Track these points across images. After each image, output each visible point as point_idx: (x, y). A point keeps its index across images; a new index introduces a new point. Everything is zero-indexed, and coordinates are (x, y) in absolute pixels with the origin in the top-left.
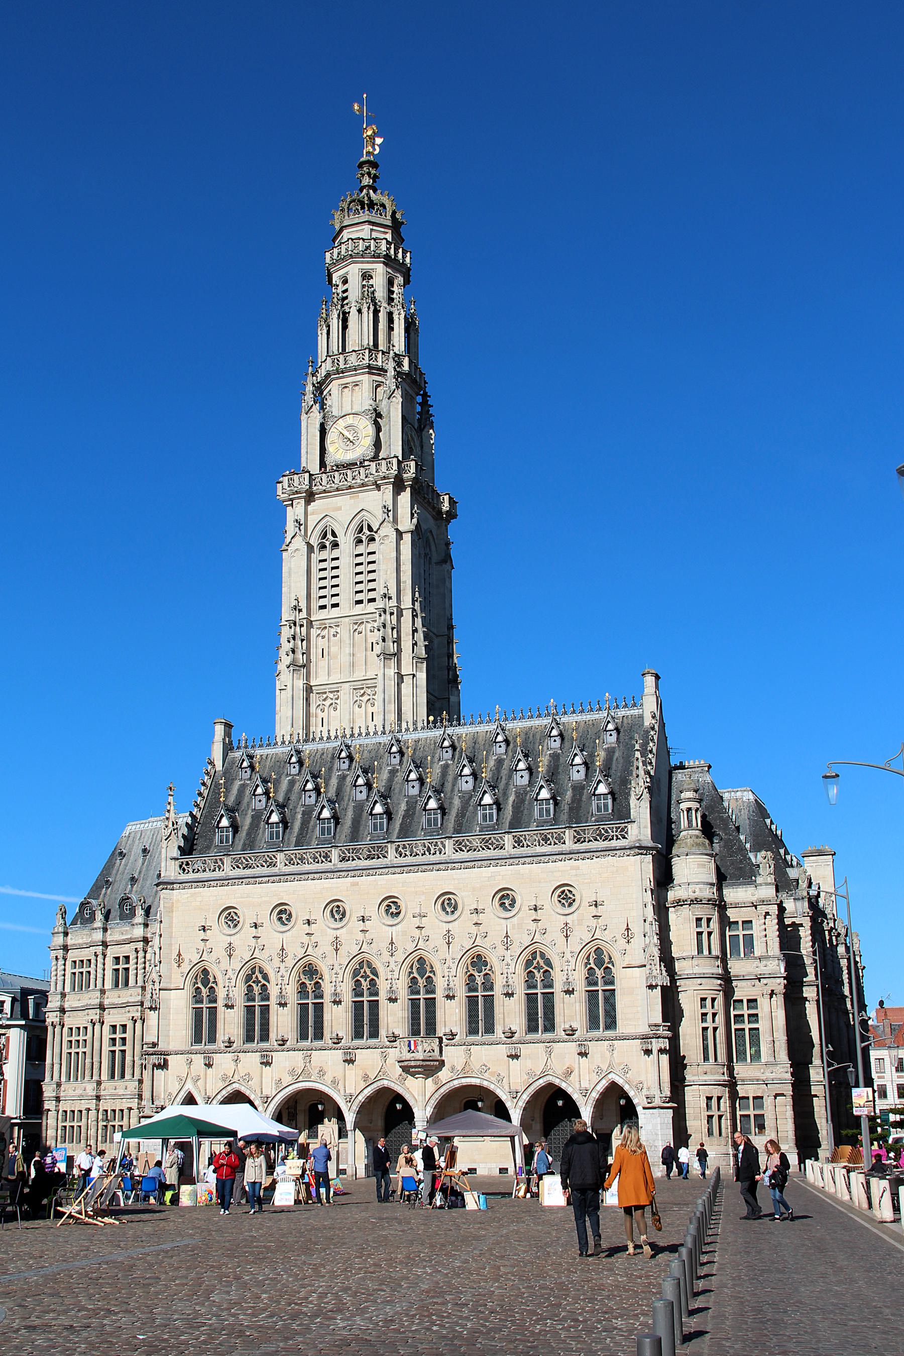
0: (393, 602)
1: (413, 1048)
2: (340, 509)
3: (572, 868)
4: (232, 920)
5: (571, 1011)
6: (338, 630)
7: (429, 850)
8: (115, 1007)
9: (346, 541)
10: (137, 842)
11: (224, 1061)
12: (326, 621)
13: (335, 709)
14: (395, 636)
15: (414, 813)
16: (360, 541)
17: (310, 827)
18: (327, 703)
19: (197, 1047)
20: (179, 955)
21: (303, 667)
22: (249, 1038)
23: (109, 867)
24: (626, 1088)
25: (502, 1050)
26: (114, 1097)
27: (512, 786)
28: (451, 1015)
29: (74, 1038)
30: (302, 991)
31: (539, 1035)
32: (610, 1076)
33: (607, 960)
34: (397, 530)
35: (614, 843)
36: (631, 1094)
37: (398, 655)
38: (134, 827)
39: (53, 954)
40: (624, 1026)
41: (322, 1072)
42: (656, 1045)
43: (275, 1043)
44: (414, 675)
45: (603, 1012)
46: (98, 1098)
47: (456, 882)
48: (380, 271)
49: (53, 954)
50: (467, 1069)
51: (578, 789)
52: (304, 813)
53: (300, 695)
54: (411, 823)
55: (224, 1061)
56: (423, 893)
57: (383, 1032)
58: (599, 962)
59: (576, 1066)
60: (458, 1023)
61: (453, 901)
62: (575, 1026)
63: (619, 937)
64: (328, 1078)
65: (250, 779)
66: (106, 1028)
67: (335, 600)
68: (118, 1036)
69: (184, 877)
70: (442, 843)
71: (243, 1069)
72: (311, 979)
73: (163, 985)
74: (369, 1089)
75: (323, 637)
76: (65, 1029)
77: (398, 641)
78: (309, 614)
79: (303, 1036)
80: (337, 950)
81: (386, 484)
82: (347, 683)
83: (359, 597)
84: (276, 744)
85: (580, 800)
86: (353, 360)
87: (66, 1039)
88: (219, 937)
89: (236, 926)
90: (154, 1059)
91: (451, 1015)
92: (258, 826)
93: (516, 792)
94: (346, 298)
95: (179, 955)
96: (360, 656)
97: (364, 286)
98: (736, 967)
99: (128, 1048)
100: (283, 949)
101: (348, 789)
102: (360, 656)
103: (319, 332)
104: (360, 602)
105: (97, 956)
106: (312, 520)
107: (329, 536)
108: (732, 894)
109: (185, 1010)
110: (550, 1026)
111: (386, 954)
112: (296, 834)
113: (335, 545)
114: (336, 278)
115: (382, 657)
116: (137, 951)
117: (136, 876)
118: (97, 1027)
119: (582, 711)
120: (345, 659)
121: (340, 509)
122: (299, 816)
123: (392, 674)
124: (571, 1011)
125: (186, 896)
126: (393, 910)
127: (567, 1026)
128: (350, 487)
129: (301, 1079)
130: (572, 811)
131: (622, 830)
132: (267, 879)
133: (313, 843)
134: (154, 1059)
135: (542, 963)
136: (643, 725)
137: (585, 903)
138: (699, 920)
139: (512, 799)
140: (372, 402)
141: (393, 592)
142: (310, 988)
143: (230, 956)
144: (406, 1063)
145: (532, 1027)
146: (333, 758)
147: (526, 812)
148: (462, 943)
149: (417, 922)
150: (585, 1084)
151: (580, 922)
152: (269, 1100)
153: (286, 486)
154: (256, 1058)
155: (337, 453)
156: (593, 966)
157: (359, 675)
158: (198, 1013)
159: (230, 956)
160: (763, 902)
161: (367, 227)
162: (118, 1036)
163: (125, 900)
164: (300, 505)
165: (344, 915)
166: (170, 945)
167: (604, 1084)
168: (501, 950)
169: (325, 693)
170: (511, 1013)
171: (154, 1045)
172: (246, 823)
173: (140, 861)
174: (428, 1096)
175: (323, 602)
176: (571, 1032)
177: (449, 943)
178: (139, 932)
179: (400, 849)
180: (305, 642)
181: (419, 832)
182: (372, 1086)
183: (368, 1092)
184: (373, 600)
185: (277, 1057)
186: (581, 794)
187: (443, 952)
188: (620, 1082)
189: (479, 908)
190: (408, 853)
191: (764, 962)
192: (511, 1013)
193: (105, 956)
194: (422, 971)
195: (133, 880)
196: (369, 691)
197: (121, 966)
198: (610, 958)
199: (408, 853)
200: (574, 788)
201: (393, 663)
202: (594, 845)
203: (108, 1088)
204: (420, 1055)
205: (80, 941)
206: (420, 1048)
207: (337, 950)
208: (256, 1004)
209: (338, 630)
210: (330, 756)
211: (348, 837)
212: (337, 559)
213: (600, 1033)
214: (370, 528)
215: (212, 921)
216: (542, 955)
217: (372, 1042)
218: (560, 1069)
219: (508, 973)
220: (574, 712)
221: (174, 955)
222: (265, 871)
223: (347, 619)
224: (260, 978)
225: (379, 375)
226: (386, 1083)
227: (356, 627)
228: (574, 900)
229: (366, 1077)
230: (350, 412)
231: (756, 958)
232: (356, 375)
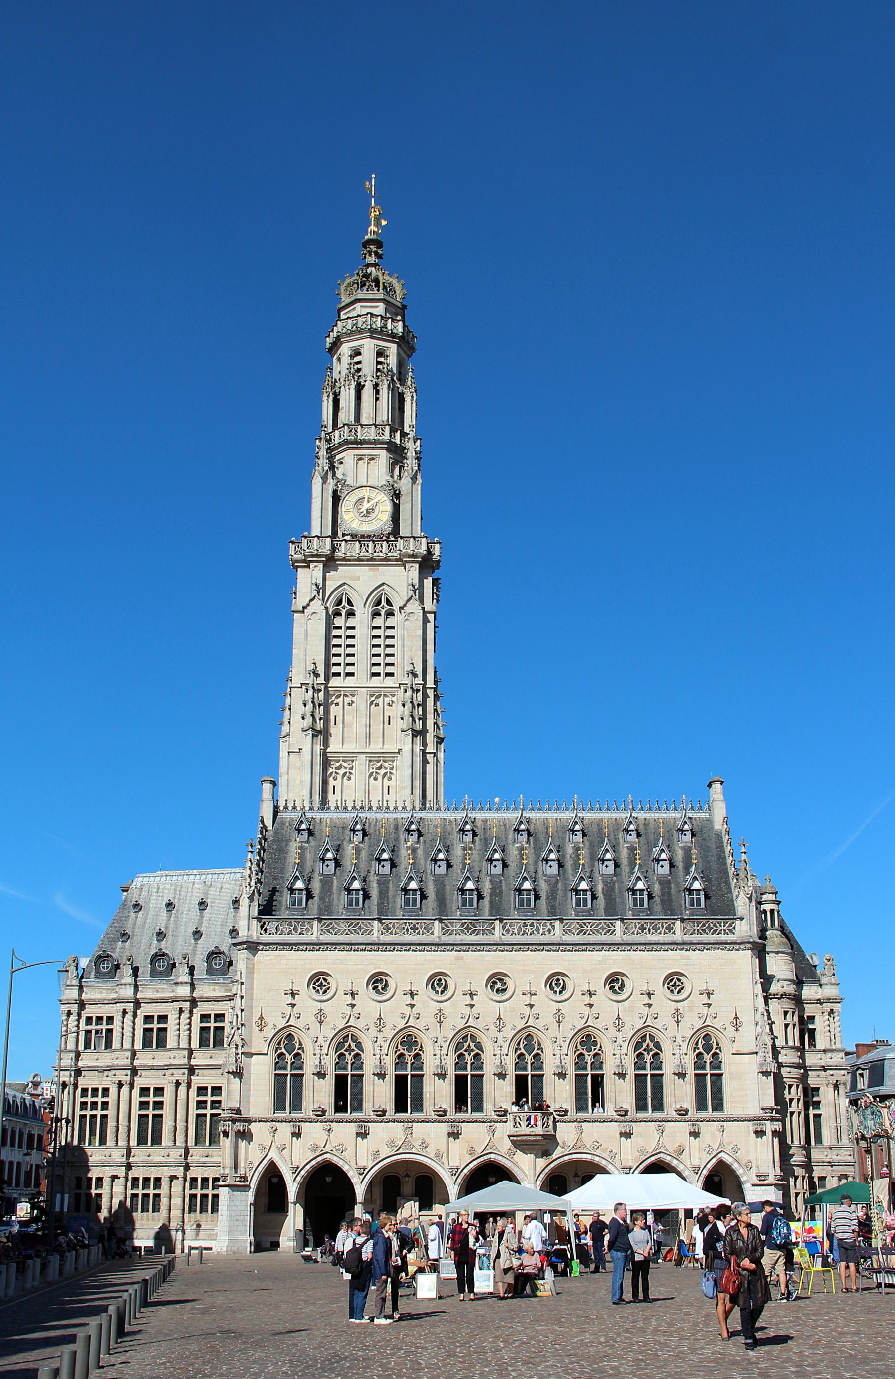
0: (419, 680)
1: (532, 1123)
2: (358, 578)
3: (683, 957)
4: (321, 985)
5: (679, 1093)
6: (354, 699)
7: (538, 930)
8: (152, 1068)
9: (363, 613)
10: (154, 896)
11: (314, 1132)
12: (341, 689)
13: (349, 779)
14: (420, 713)
15: (501, 892)
16: (376, 614)
17: (390, 897)
18: (341, 771)
19: (280, 1115)
20: (261, 1018)
21: (322, 734)
22: (340, 1108)
23: (122, 918)
24: (735, 1166)
25: (615, 1128)
26: (148, 1165)
27: (597, 874)
28: (559, 1093)
29: (89, 1100)
30: (400, 1060)
31: (649, 1114)
32: (720, 1155)
33: (715, 1046)
34: (423, 609)
35: (723, 937)
36: (740, 1171)
37: (423, 733)
38: (146, 879)
39: (65, 1008)
40: (730, 1108)
41: (424, 1145)
42: (769, 1127)
43: (372, 1114)
45: (710, 1092)
46: (129, 1167)
47: (566, 962)
48: (393, 349)
49: (65, 1008)
50: (579, 1144)
51: (665, 883)
52: (379, 881)
53: (318, 760)
54: (500, 902)
55: (314, 1132)
56: (533, 972)
57: (488, 1106)
58: (708, 1047)
59: (687, 1143)
60: (569, 1100)
61: (561, 981)
62: (685, 1106)
63: (728, 1025)
64: (431, 1151)
65: (308, 842)
66: (136, 1092)
67: (349, 669)
68: (151, 1099)
69: (265, 938)
70: (551, 924)
71: (335, 1140)
72: (409, 1050)
73: (245, 1049)
74: (475, 1162)
76: (79, 1091)
77: (424, 719)
78: (327, 679)
79: (401, 1106)
80: (440, 1022)
81: (412, 562)
82: (362, 755)
83: (376, 669)
84: (329, 808)
85: (669, 894)
86: (372, 434)
87: (79, 1100)
88: (308, 1002)
90: (239, 1126)
91: (559, 1093)
92: (330, 890)
93: (603, 882)
94: (359, 370)
95: (261, 1018)
96: (377, 728)
97: (379, 363)
98: (812, 1059)
99: (167, 1112)
100: (380, 1019)
101: (422, 862)
102: (377, 728)
103: (325, 398)
104: (378, 674)
105: (125, 1012)
106: (330, 586)
108: (809, 992)
109: (267, 1077)
110: (659, 1106)
111: (493, 1029)
112: (376, 903)
113: (351, 614)
114: (345, 349)
115: (410, 732)
116: (181, 1011)
118: (125, 1090)
119: (650, 809)
120: (362, 730)
121: (358, 578)
122: (375, 885)
123: (418, 750)
124: (679, 1093)
126: (499, 985)
127: (678, 1107)
128: (372, 559)
129: (401, 1151)
130: (664, 904)
131: (730, 925)
133: (398, 914)
134: (239, 1126)
135: (651, 1045)
136: (712, 828)
137: (696, 992)
138: (786, 1013)
139: (600, 887)
140: (389, 478)
141: (419, 670)
142: (409, 1059)
143: (321, 1022)
144: (515, 1138)
145: (641, 1106)
146: (397, 828)
147: (617, 900)
148: (573, 1023)
149: (527, 1000)
150: (696, 1163)
151: (690, 1009)
152: (367, 1171)
153: (305, 547)
154: (353, 1128)
155: (350, 520)
156: (701, 1050)
157: (376, 747)
158: (280, 1079)
159: (321, 1022)
160: (829, 1000)
161: (382, 306)
162: (151, 1099)
163: (159, 956)
164: (317, 571)
165: (446, 988)
166: (251, 1007)
167: (714, 1160)
168: (612, 1031)
169: (338, 761)
170: (620, 1093)
171: (238, 1111)
172: (316, 887)
173: (164, 915)
174: (538, 1170)
176: (683, 1113)
177: (559, 1022)
178: (184, 991)
179: (507, 927)
180: (322, 708)
181: (512, 911)
182: (479, 1160)
183: (472, 1165)
184: (392, 674)
185: (375, 1128)
186: (669, 889)
187: (554, 1030)
188: (728, 1159)
189: (354, 989)
190: (515, 931)
191: (829, 1055)
192: (620, 1093)
193: (135, 1015)
194: (529, 1048)
195: (161, 935)
196: (386, 765)
197: (155, 1026)
198: (718, 1044)
199: (515, 931)
200: (661, 883)
201: (418, 740)
202: (704, 938)
203: (140, 1154)
204: (539, 1130)
205: (98, 996)
206: (539, 1123)
207: (440, 1022)
208: (349, 1072)
209: (354, 699)
210: (392, 826)
211: (436, 911)
212: (353, 628)
213: (709, 1113)
214: (389, 603)
215: (301, 985)
216: (652, 1037)
217: (477, 1115)
218: (672, 1148)
219: (616, 1055)
220: (642, 809)
221: (255, 1018)
223: (365, 690)
224: (353, 1047)
226: (492, 1156)
227: (373, 699)
228: (682, 988)
229: (472, 1151)
230: (365, 484)
231: (820, 1051)
232: (373, 448)
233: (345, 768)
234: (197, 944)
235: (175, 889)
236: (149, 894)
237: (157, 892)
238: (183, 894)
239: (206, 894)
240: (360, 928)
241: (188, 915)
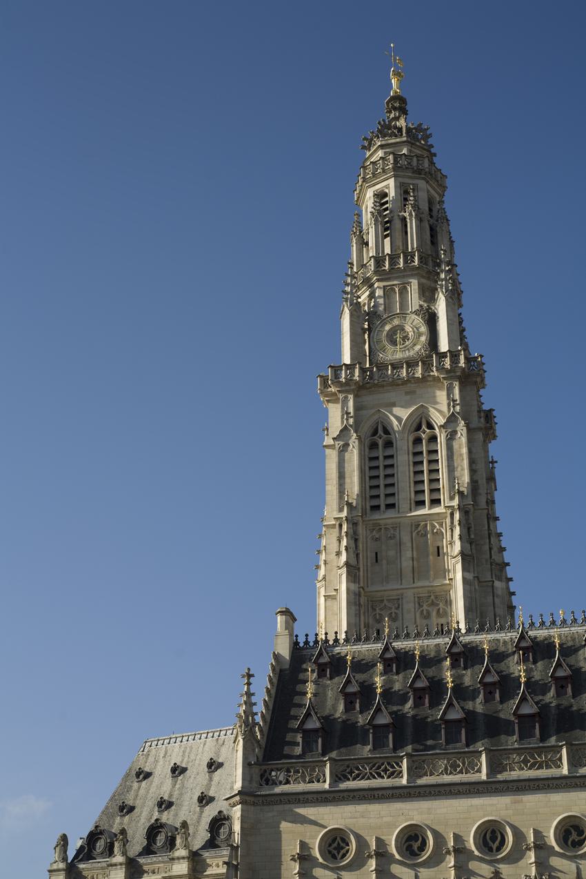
10: (161, 762)
23: (124, 788)
44: (493, 581)
67: (390, 501)
75: (377, 539)
83: (420, 498)
89: (344, 855)
107: (380, 432)
113: (389, 444)
117: (166, 798)
125: (270, 814)
132: (390, 792)
173: (169, 781)
175: (375, 502)
195: (164, 805)
222: (386, 782)
225: (428, 278)
233: (390, 608)
234: (202, 812)
235: (184, 752)
236: (156, 761)
237: (164, 757)
238: (192, 757)
239: (218, 753)
240: (386, 770)
241: (196, 781)
